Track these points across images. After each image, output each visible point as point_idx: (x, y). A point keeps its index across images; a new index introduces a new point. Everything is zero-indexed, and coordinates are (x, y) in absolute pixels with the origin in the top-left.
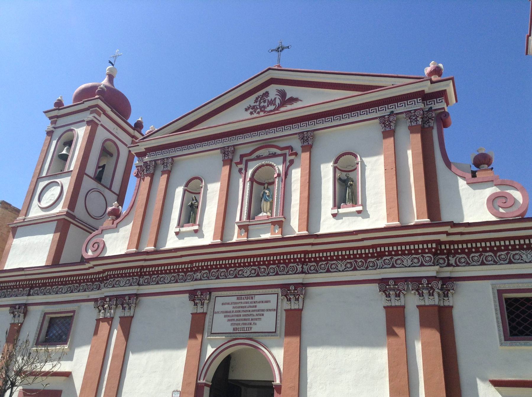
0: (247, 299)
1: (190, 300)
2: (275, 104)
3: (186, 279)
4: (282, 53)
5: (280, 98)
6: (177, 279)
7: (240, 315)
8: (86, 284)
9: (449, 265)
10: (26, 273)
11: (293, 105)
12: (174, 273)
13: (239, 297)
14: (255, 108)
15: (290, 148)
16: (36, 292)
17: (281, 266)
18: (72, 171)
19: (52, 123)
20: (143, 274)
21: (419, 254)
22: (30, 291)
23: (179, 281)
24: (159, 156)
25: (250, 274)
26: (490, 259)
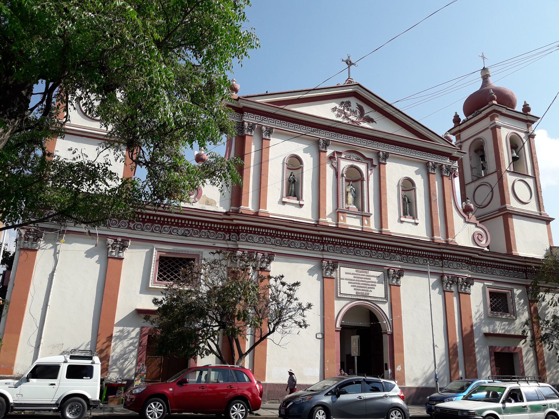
8: (208, 231)
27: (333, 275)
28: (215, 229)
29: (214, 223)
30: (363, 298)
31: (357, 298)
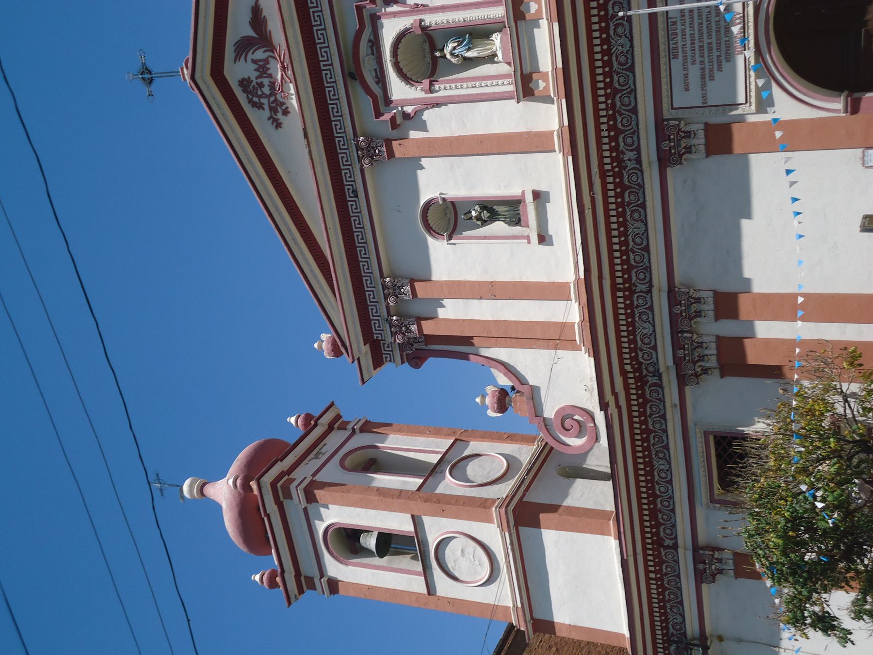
0: (676, 34)
1: (680, 163)
2: (266, 61)
3: (636, 185)
4: (154, 70)
5: (254, 48)
7: (710, 44)
8: (650, 416)
10: (632, 553)
11: (268, 17)
12: (626, 214)
13: (672, 54)
14: (274, 105)
15: (359, 9)
16: (668, 531)
18: (413, 517)
19: (312, 586)
20: (627, 285)
22: (668, 547)
23: (641, 201)
24: (379, 308)
25: (625, 35)
29: (630, 412)
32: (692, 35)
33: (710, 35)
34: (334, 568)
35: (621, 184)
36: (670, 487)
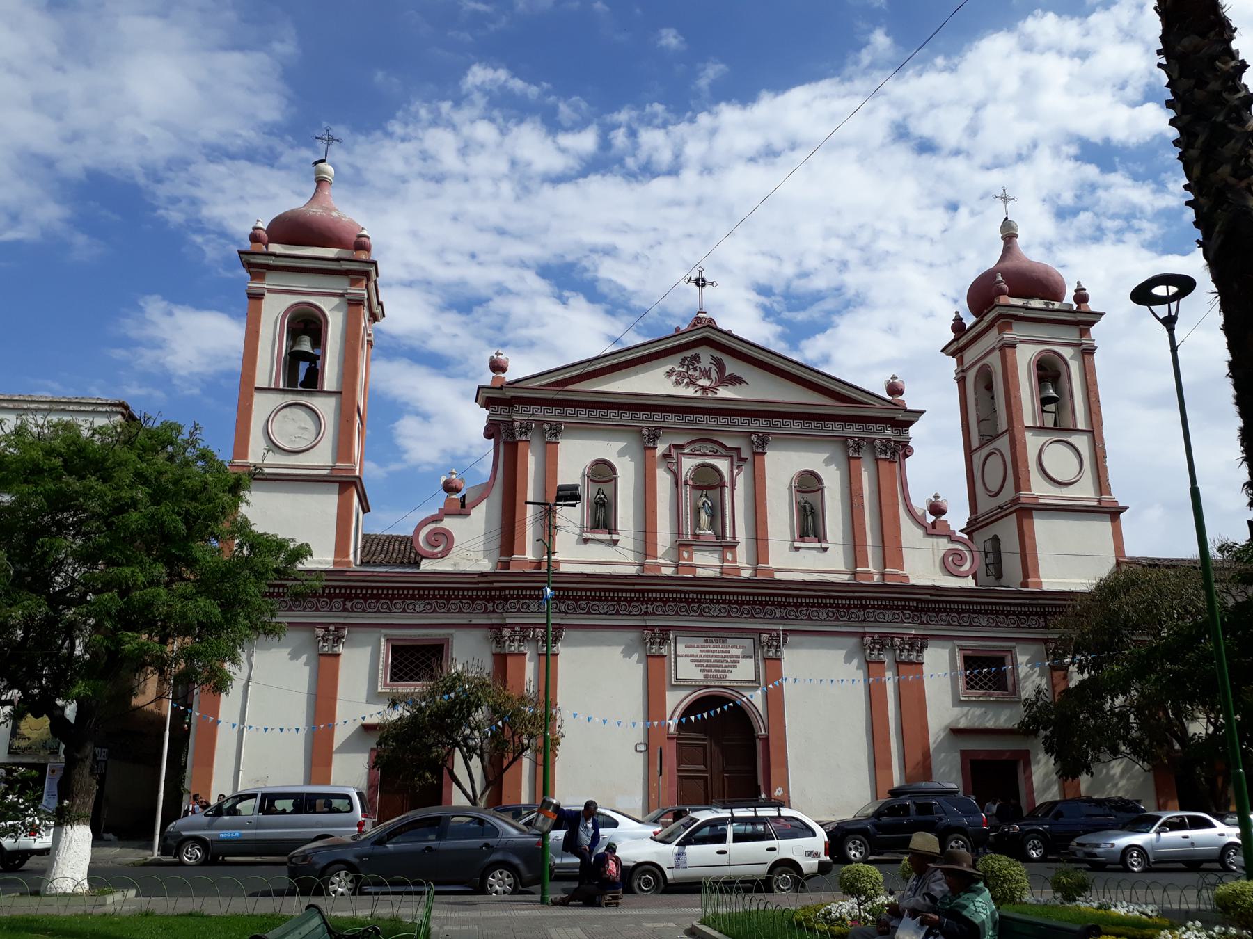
6: (617, 610)
9: (922, 623)
17: (757, 607)
21: (899, 610)
26: (955, 619)
27: (662, 651)
28: (470, 598)
29: (468, 589)
30: (717, 684)
31: (705, 684)
32: (715, 652)
33: (715, 661)
34: (275, 309)
35: (632, 600)
36: (400, 611)
